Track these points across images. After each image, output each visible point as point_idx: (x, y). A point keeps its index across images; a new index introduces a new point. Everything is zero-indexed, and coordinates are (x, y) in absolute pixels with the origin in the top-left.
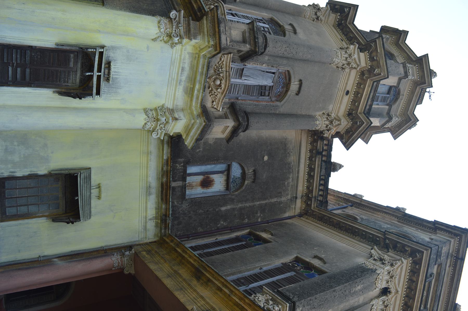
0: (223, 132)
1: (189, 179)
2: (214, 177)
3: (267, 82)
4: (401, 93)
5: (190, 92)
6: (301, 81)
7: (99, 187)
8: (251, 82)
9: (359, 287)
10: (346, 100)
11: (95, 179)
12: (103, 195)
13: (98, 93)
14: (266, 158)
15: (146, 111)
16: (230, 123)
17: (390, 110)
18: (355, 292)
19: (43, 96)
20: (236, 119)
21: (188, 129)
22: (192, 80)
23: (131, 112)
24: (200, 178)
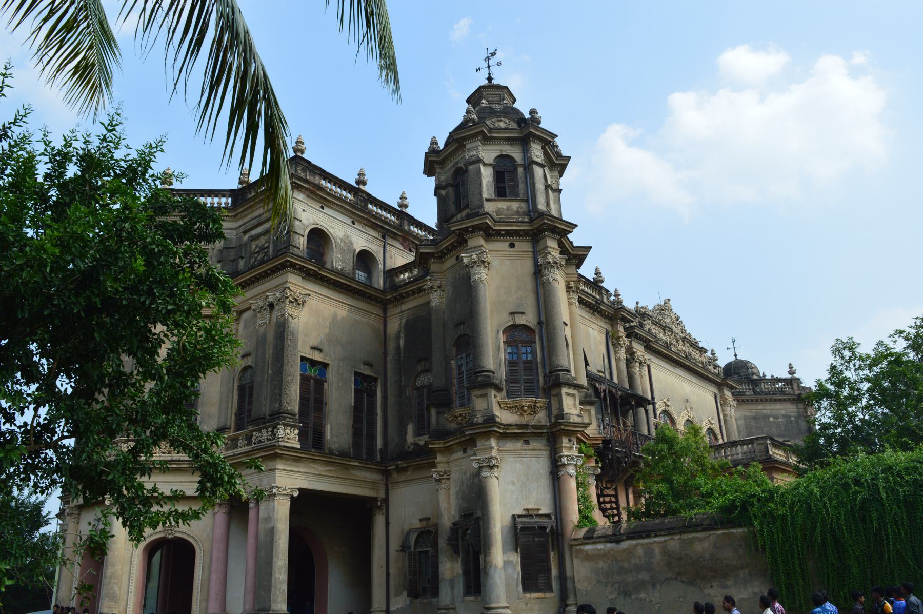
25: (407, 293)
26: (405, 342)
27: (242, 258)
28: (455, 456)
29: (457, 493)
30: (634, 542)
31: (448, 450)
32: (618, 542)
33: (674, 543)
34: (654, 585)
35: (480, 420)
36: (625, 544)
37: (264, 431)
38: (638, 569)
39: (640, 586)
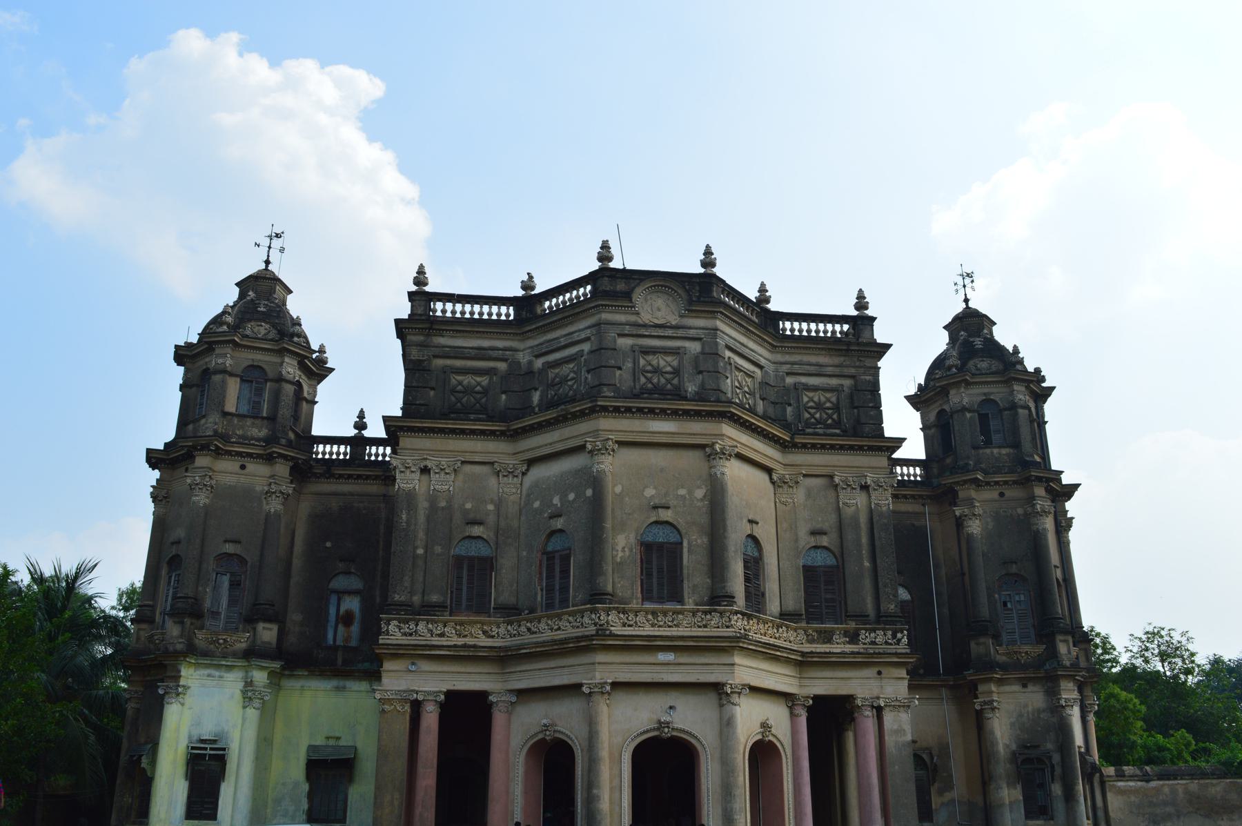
0: (270, 629)
1: (339, 642)
2: (343, 609)
3: (225, 581)
4: (250, 363)
5: (230, 668)
6: (226, 541)
7: (328, 738)
8: (224, 602)
9: (404, 516)
10: (252, 467)
11: (320, 741)
12: (337, 735)
13: (224, 749)
14: (328, 544)
15: (244, 707)
16: (261, 626)
17: (271, 380)
18: (408, 522)
19: (226, 791)
20: (257, 621)
21: (262, 668)
22: (218, 667)
23: (244, 719)
24: (341, 628)
27: (790, 405)
28: (1007, 688)
29: (1012, 725)
31: (1000, 682)
32: (1147, 781)
33: (1194, 785)
34: (1179, 817)
35: (1068, 663)
36: (1154, 784)
37: (881, 633)
38: (1165, 804)
39: (1169, 817)
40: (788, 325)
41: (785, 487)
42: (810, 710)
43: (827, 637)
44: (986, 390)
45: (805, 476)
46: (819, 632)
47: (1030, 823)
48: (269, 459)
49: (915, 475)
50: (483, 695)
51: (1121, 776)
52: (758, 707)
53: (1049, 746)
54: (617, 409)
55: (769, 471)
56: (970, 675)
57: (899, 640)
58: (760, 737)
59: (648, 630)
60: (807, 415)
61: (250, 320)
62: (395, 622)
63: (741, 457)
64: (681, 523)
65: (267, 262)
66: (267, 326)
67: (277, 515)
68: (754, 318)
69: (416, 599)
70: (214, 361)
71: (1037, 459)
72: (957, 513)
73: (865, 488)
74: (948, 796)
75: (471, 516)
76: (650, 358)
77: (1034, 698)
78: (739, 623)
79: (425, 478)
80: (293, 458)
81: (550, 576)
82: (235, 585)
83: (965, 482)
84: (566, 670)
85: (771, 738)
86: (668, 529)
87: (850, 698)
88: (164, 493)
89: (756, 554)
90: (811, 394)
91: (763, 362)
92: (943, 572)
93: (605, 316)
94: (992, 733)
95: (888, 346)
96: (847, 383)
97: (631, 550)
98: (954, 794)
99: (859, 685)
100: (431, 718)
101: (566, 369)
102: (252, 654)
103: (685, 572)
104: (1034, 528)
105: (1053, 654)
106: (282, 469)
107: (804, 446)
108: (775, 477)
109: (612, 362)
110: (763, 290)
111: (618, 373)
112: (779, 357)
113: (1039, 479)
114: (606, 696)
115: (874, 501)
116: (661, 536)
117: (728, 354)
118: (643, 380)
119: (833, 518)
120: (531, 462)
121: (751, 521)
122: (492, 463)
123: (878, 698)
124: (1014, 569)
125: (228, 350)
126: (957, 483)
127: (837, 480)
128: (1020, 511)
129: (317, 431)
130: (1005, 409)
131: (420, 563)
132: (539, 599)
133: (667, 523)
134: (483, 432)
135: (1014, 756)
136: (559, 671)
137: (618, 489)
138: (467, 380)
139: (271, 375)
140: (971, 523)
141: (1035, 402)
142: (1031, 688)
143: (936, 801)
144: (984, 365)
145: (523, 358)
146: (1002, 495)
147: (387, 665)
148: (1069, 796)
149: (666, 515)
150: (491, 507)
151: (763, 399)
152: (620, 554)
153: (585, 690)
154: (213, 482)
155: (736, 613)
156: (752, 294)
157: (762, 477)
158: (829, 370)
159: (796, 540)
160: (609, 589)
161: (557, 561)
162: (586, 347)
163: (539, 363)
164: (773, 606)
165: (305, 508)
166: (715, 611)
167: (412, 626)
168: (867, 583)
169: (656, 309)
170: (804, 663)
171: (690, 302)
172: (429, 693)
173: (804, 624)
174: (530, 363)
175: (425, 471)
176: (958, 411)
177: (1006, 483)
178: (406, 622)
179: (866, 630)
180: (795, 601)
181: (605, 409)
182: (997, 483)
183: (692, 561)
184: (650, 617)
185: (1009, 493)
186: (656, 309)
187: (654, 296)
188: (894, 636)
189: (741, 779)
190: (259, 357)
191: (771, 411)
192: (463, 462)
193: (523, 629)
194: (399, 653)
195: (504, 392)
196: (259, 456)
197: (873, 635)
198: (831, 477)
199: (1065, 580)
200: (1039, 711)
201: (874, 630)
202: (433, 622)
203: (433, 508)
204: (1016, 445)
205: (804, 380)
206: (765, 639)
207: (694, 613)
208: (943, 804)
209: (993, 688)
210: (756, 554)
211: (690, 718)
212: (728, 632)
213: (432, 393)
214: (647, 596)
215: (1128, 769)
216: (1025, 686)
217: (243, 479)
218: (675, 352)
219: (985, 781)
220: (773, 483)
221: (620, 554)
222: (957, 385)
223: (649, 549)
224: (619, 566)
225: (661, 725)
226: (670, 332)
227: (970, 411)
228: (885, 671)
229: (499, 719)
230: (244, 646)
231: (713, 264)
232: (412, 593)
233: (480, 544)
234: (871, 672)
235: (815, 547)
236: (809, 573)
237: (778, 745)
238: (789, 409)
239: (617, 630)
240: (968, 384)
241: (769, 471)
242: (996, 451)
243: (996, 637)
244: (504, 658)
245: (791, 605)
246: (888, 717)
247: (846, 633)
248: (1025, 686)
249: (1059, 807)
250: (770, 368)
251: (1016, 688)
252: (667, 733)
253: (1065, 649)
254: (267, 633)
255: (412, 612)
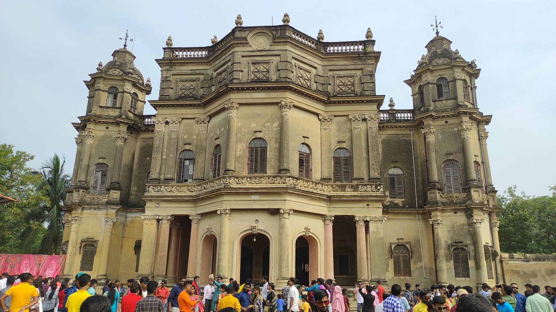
3: (99, 175)
10: (111, 128)
16: (112, 191)
25: (387, 127)
26: (383, 150)
27: (330, 84)
29: (449, 231)
30: (536, 262)
31: (443, 211)
36: (531, 263)
40: (332, 48)
41: (326, 121)
42: (334, 222)
43: (343, 188)
44: (441, 73)
45: (335, 116)
46: (339, 186)
47: (458, 279)
48: (118, 124)
49: (407, 117)
50: (187, 216)
51: (512, 258)
52: (302, 220)
53: (468, 242)
54: (238, 89)
55: (317, 115)
56: (427, 208)
57: (379, 190)
58: (304, 233)
59: (248, 185)
60: (338, 89)
61: (111, 68)
62: (152, 187)
63: (295, 106)
64: (267, 138)
65: (125, 46)
66: (119, 70)
67: (122, 148)
68: (313, 46)
69: (162, 177)
70: (97, 85)
71: (470, 106)
72: (423, 132)
73: (364, 120)
74: (419, 265)
75: (186, 141)
76: (256, 66)
77: (460, 219)
78: (290, 182)
79: (167, 126)
80: (127, 123)
81: (215, 165)
82: (104, 175)
83: (427, 117)
84: (214, 204)
85: (311, 234)
86: (261, 141)
87: (353, 217)
88: (80, 141)
89: (308, 152)
90: (341, 79)
91: (316, 65)
92: (419, 161)
93: (236, 49)
94: (437, 235)
95: (380, 53)
96: (359, 73)
97: (244, 151)
98: (423, 264)
99: (358, 211)
100: (166, 226)
101: (224, 74)
102: (109, 203)
103: (268, 159)
104: (462, 137)
105: (470, 197)
106: (124, 128)
107: (335, 102)
108: (320, 117)
109: (239, 69)
110: (320, 33)
111: (241, 73)
112: (326, 63)
113: (465, 113)
114: (228, 215)
115: (369, 125)
116: (258, 144)
117: (294, 61)
118: (253, 76)
119: (348, 135)
120: (211, 117)
121: (303, 137)
122: (195, 118)
123: (366, 217)
124: (451, 157)
125: (101, 81)
126: (423, 118)
127: (350, 117)
128: (456, 129)
129: (145, 113)
130: (450, 81)
131: (164, 161)
132: (211, 174)
133: (261, 138)
134: (191, 105)
135: (449, 247)
136: (212, 205)
137: (239, 125)
138: (188, 84)
139: (120, 90)
140: (429, 136)
141: (470, 78)
142: (459, 213)
143: (413, 267)
144: (440, 61)
145: (210, 72)
146: (446, 122)
147: (148, 204)
148: (478, 267)
149: (259, 135)
150: (195, 137)
151: (316, 82)
152: (239, 153)
153: (218, 212)
154: (94, 135)
155: (289, 177)
156: (315, 37)
157: (315, 118)
158: (350, 67)
159: (330, 146)
160: (232, 168)
161: (218, 158)
162: (230, 64)
163: (215, 74)
164: (316, 175)
165: (139, 144)
166: (278, 176)
167: (159, 188)
168: (364, 164)
169: (259, 43)
170: (330, 199)
171: (274, 39)
172: (164, 216)
173: (332, 183)
174: (212, 74)
175: (167, 123)
176: (426, 84)
177: (448, 116)
178: (156, 186)
179: (362, 185)
180: (329, 172)
181: (232, 89)
182: (443, 117)
183: (271, 154)
184: (249, 180)
185: (451, 121)
186: (259, 43)
187: (259, 38)
188: (376, 187)
189: (290, 251)
190: (114, 83)
191: (320, 88)
192: (182, 119)
193: (203, 188)
194: (152, 199)
195: (202, 88)
196: (113, 123)
197: (365, 188)
198: (348, 116)
199: (482, 163)
200: (463, 225)
201: (366, 185)
202: (167, 186)
203: (170, 139)
204: (456, 98)
205: (337, 72)
206: (306, 189)
207: (269, 177)
208: (417, 268)
209: (438, 213)
210: (308, 152)
211: (265, 225)
212: (284, 186)
213: (171, 91)
214: (250, 172)
215: (516, 255)
216: (456, 213)
217: (107, 133)
218: (267, 63)
219: (436, 257)
220: (320, 120)
221: (239, 153)
222: (425, 72)
223: (252, 150)
224: (237, 158)
225: (253, 228)
226: (265, 53)
227: (432, 84)
228: (371, 205)
229: (194, 226)
230: (106, 200)
231: (288, 21)
232: (160, 174)
233: (190, 153)
234: (364, 205)
235: (339, 148)
236: (337, 160)
237: (316, 238)
238: (329, 87)
239: (234, 186)
240: (432, 71)
241: (317, 115)
242: (444, 102)
243: (440, 190)
244: (195, 200)
245: (326, 175)
246: (372, 226)
247: (352, 187)
248: (456, 213)
249: (472, 271)
250: (320, 68)
251: (452, 214)
252: (255, 232)
253: (477, 196)
254: (116, 195)
255: (158, 182)
